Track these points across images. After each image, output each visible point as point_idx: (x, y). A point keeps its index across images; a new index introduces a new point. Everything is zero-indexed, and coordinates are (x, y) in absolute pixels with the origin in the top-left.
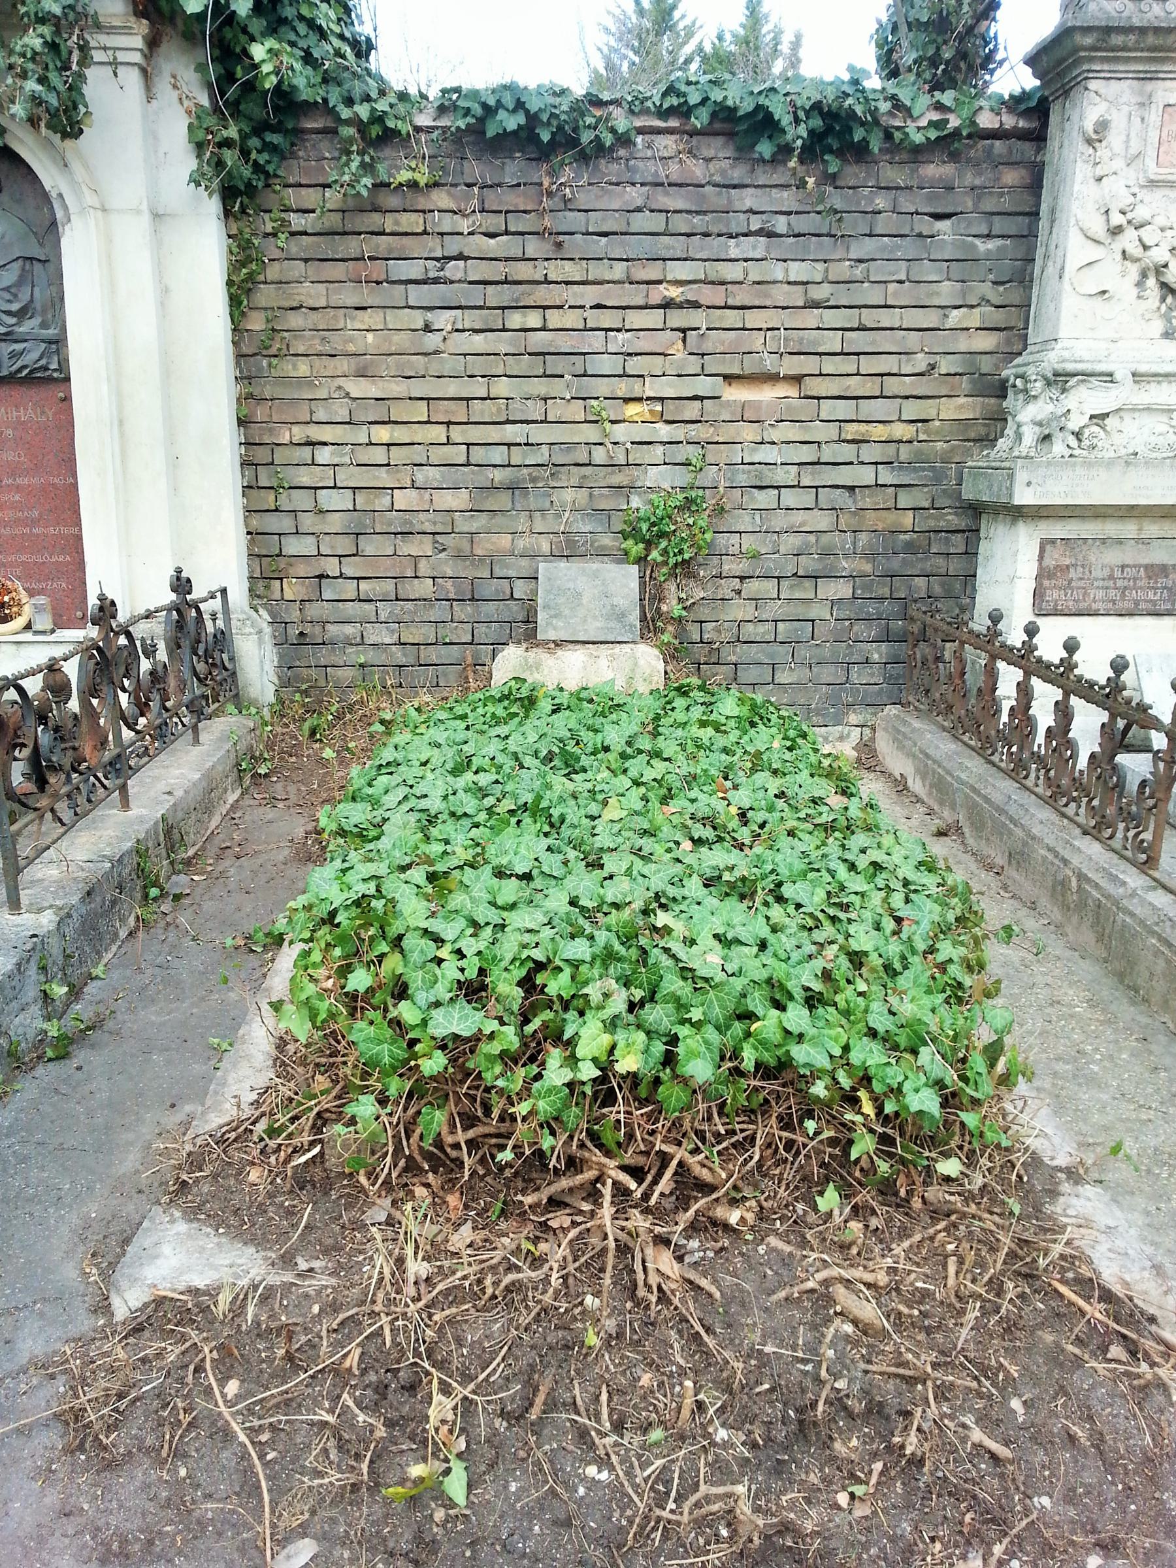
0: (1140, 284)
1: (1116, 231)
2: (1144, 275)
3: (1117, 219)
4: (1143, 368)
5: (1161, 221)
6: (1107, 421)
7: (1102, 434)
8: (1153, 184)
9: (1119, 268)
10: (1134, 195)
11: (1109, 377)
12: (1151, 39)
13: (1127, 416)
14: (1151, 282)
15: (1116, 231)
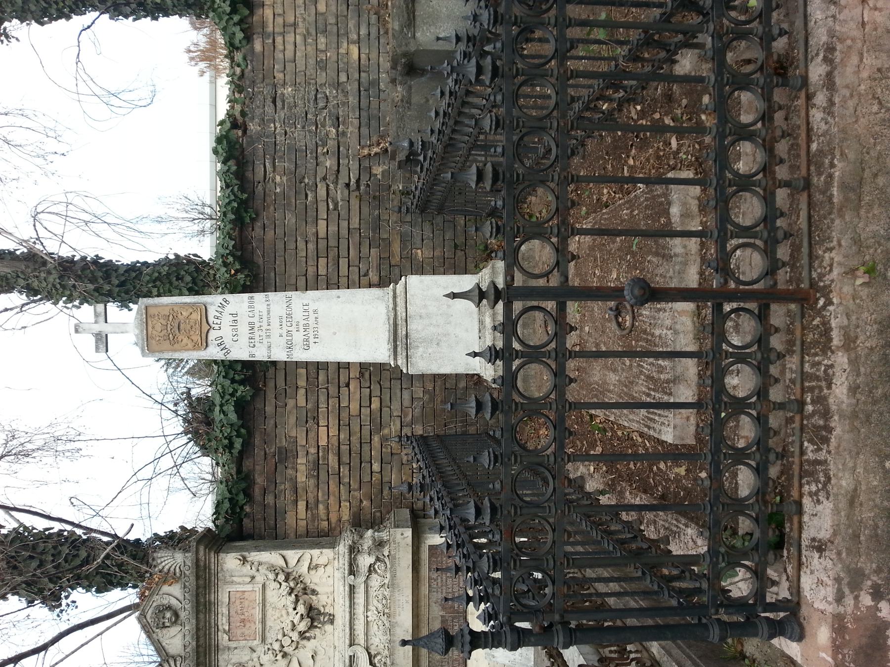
0: (309, 639)
1: (285, 655)
2: (305, 638)
3: (279, 657)
4: (347, 642)
5: (280, 637)
6: (373, 653)
7: (379, 657)
8: (263, 640)
9: (301, 650)
10: (269, 649)
11: (352, 659)
12: (202, 659)
13: (370, 642)
14: (307, 635)
15: (285, 655)
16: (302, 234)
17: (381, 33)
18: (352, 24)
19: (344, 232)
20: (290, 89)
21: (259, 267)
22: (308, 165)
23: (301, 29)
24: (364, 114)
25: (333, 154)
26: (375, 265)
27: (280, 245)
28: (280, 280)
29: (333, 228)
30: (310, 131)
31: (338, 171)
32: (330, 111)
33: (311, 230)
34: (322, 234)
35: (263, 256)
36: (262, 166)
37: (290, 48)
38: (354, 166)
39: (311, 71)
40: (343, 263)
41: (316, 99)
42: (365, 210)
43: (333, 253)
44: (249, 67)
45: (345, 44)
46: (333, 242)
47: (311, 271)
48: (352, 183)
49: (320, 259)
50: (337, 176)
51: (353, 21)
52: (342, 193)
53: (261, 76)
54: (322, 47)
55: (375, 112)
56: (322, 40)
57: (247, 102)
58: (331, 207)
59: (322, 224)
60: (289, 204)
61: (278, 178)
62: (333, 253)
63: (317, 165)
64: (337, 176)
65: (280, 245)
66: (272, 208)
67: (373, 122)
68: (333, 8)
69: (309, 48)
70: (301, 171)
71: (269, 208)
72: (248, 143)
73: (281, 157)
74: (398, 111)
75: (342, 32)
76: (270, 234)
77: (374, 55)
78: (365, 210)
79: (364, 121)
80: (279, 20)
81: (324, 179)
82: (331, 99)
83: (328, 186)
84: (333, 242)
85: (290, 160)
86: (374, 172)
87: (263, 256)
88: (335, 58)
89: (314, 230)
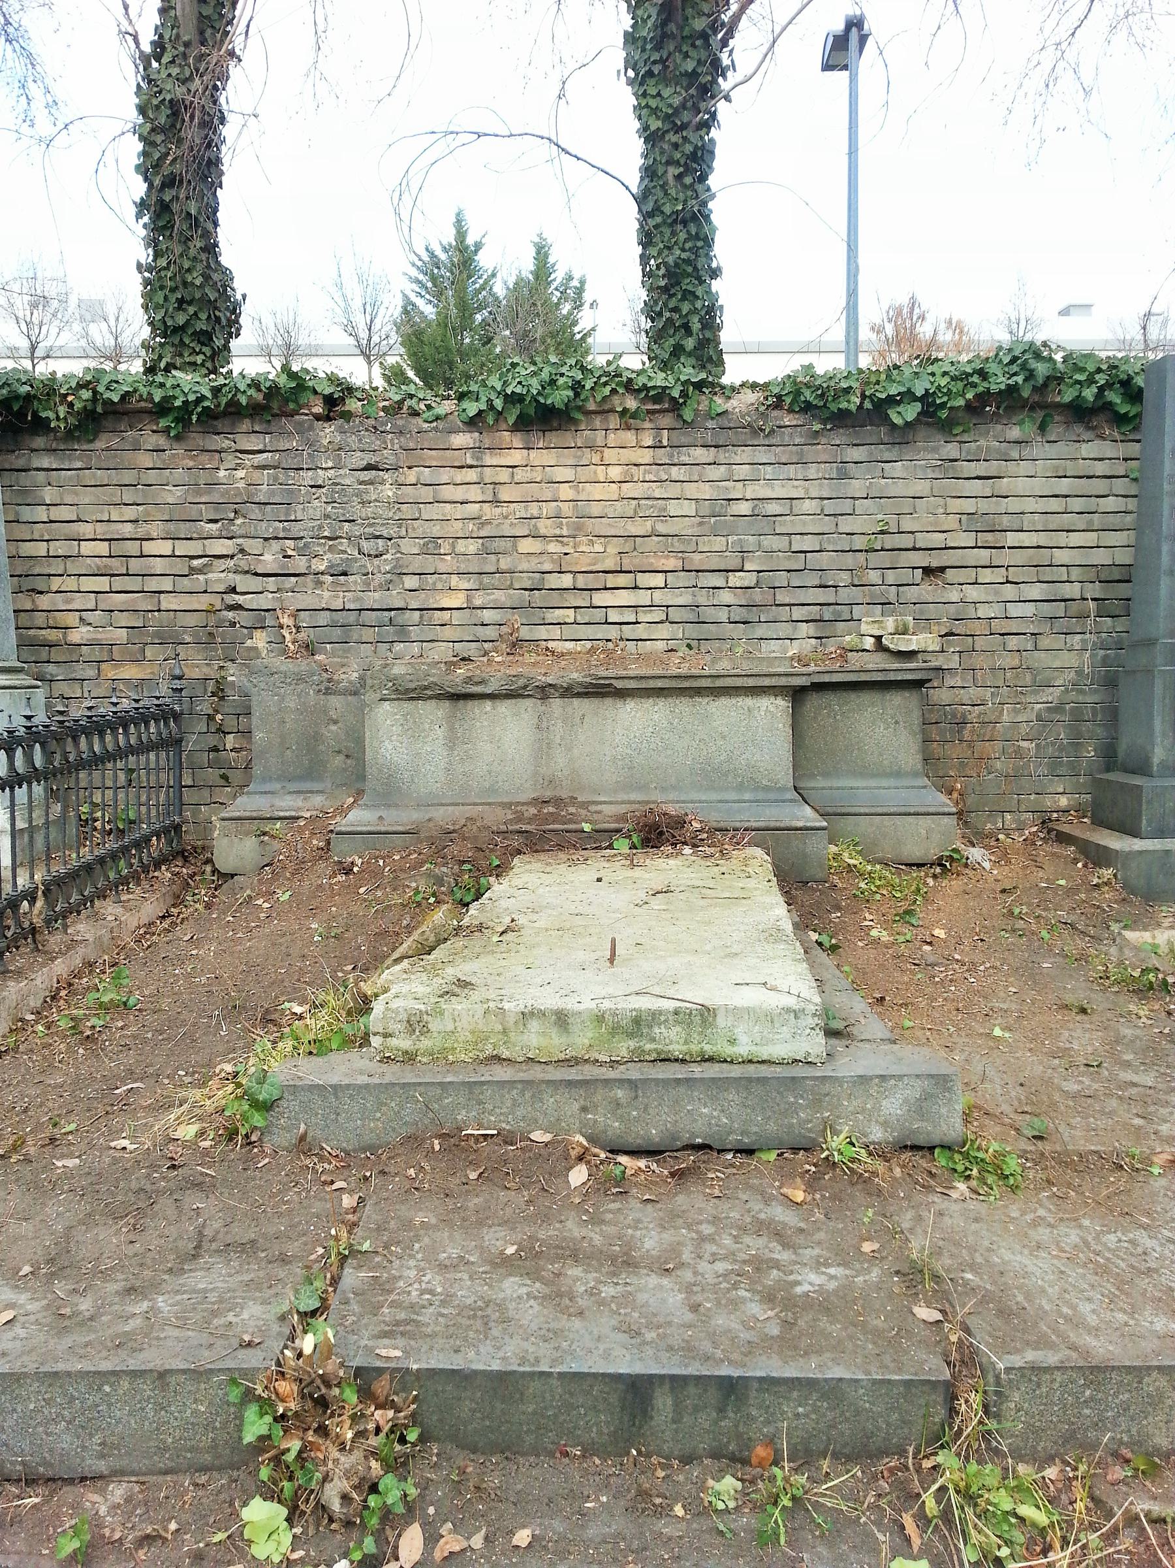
16: (148, 513)
17: (486, 645)
18: (500, 596)
19: (153, 584)
20: (390, 494)
21: (91, 441)
22: (264, 525)
23: (488, 511)
24: (352, 617)
25: (283, 567)
26: (99, 636)
27: (128, 477)
28: (70, 478)
29: (159, 566)
30: (321, 527)
31: (256, 574)
32: (356, 560)
33: (155, 529)
34: (149, 548)
35: (108, 449)
36: (261, 447)
37: (459, 493)
38: (265, 601)
39: (420, 528)
40: (102, 583)
41: (378, 537)
42: (191, 620)
43: (117, 565)
44: (427, 425)
45: (466, 586)
46: (135, 565)
47: (86, 530)
48: (237, 597)
49: (106, 543)
50: (247, 572)
51: (503, 599)
52: (219, 580)
53: (412, 445)
54: (461, 546)
55: (355, 637)
56: (472, 547)
57: (371, 422)
58: (195, 563)
59: (165, 547)
60: (199, 493)
61: (241, 474)
62: (117, 565)
63: (266, 539)
64: (247, 572)
65: (128, 477)
66: (191, 464)
67: (339, 631)
68: (524, 566)
69: (460, 524)
70: (255, 512)
71: (192, 458)
72: (301, 423)
73: (276, 478)
74: (313, 675)
75: (486, 579)
76: (146, 460)
77: (447, 633)
78: (191, 620)
79: (340, 617)
80: (504, 475)
81: (242, 551)
82: (376, 561)
83: (232, 557)
84: (135, 565)
85: (273, 493)
86: (258, 634)
87: (108, 449)
88: (442, 568)
89: (155, 535)
